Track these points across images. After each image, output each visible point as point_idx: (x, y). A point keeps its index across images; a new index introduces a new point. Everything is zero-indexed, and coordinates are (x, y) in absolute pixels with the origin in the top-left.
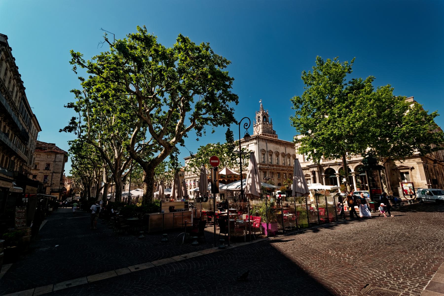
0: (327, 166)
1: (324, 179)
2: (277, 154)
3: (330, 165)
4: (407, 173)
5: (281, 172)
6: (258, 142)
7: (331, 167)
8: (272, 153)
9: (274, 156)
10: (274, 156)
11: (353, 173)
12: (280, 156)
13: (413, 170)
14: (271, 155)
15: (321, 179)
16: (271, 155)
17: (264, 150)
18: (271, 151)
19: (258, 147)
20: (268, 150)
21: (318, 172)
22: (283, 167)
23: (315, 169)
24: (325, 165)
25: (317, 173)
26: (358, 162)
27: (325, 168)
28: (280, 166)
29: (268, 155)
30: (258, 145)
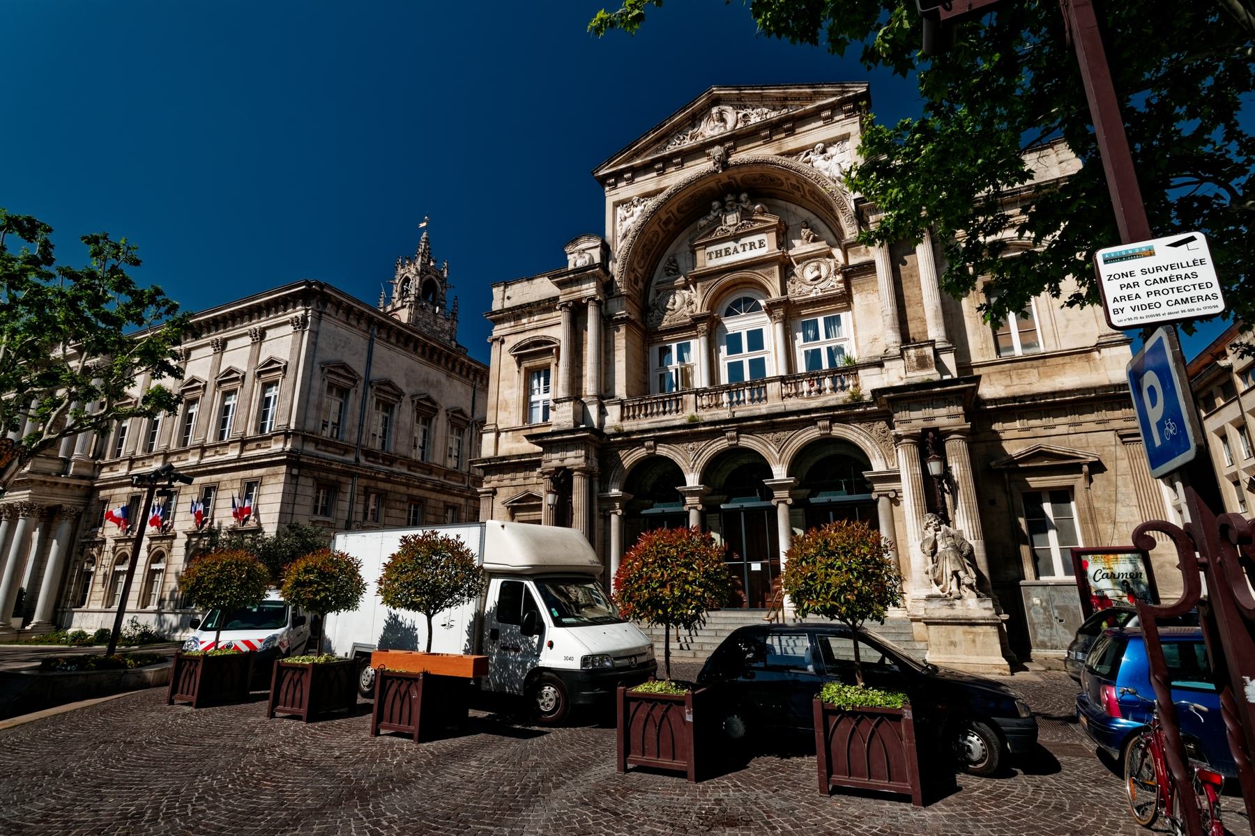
0: (640, 443)
1: (614, 519)
2: (426, 410)
3: (659, 440)
4: (1062, 496)
5: (434, 495)
6: (318, 318)
7: (662, 450)
8: (399, 394)
9: (405, 414)
10: (405, 414)
11: (781, 487)
12: (441, 423)
13: (1096, 477)
14: (388, 407)
15: (598, 522)
16: (388, 407)
17: (344, 366)
18: (389, 383)
19: (313, 345)
20: (376, 374)
21: (586, 473)
22: (448, 473)
23: (574, 459)
24: (630, 440)
25: (578, 482)
26: (813, 422)
27: (628, 459)
28: (430, 469)
29: (371, 402)
30: (314, 334)
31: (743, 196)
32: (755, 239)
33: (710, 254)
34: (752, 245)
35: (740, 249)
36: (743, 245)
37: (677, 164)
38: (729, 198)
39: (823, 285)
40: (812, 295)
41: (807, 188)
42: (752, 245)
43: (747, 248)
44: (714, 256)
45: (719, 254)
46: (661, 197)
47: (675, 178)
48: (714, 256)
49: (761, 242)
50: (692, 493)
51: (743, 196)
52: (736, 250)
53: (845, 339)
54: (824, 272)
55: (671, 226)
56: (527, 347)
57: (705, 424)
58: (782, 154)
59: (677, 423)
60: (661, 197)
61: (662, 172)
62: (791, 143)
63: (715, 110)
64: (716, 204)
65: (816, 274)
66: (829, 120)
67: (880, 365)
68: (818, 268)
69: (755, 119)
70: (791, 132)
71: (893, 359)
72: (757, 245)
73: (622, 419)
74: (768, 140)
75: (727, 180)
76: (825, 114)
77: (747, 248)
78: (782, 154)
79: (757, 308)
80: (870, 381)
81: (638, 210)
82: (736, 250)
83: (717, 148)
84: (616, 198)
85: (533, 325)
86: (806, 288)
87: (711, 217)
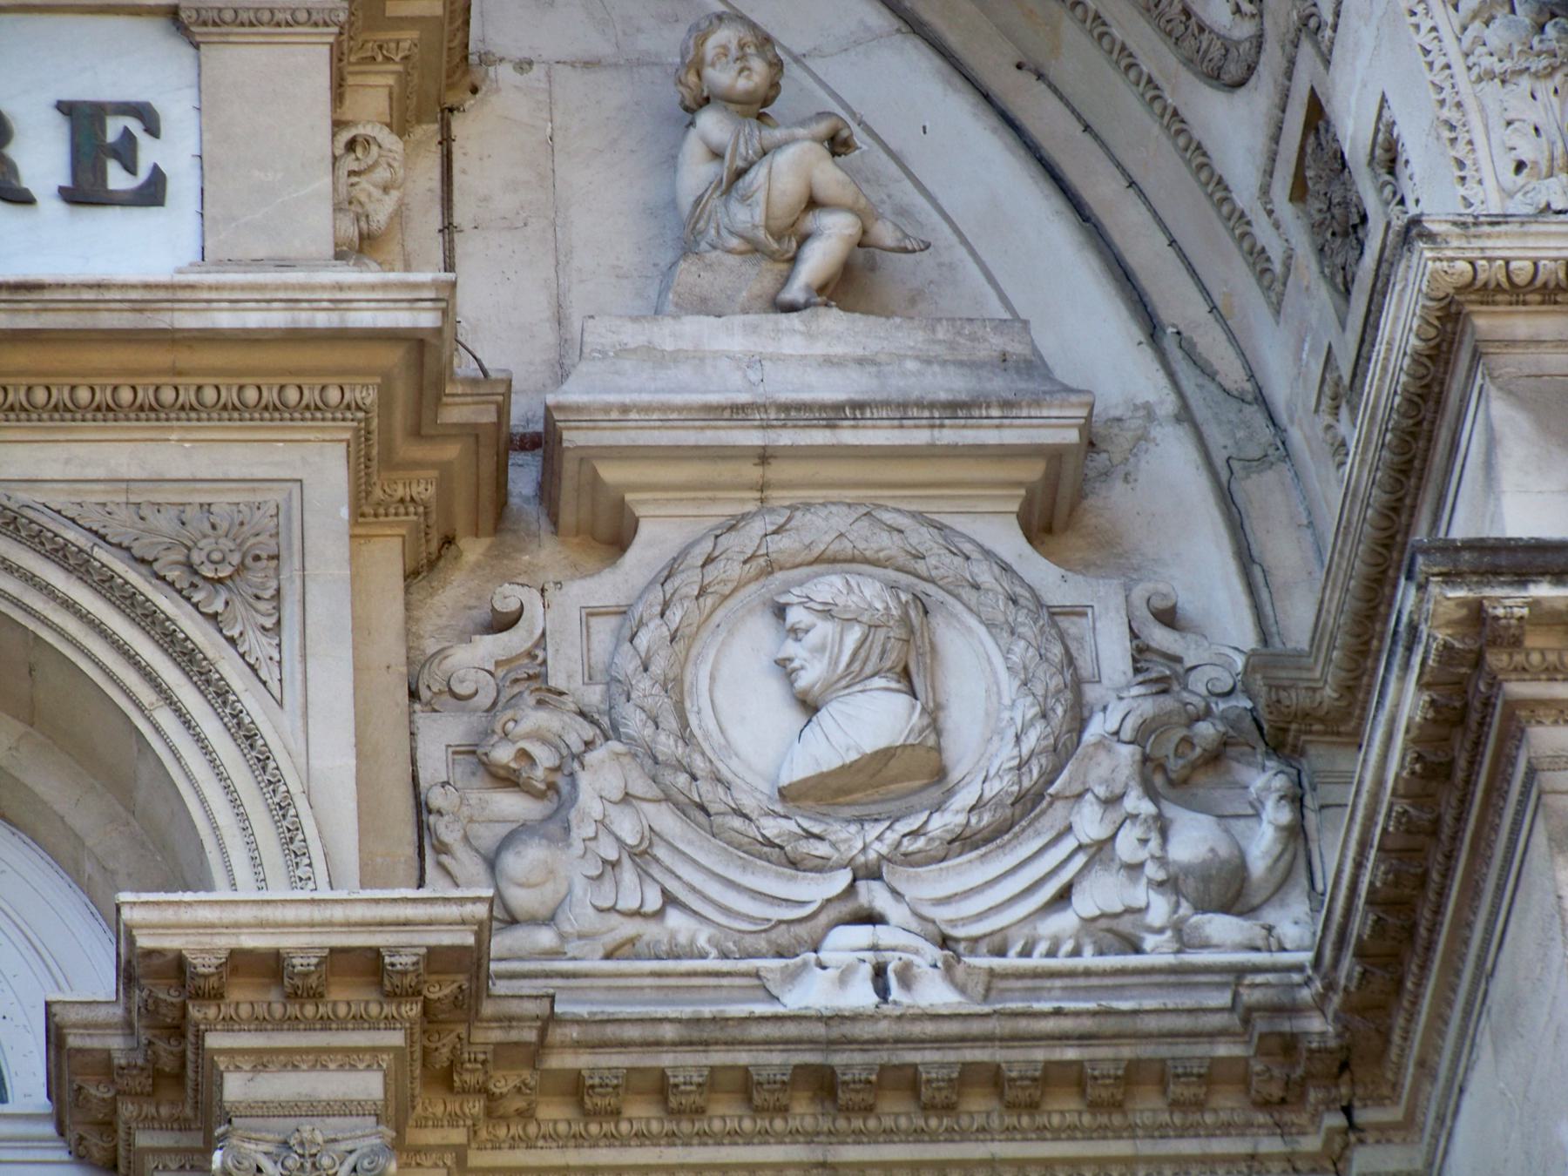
54: (986, 704)
65: (872, 720)
86: (729, 895)
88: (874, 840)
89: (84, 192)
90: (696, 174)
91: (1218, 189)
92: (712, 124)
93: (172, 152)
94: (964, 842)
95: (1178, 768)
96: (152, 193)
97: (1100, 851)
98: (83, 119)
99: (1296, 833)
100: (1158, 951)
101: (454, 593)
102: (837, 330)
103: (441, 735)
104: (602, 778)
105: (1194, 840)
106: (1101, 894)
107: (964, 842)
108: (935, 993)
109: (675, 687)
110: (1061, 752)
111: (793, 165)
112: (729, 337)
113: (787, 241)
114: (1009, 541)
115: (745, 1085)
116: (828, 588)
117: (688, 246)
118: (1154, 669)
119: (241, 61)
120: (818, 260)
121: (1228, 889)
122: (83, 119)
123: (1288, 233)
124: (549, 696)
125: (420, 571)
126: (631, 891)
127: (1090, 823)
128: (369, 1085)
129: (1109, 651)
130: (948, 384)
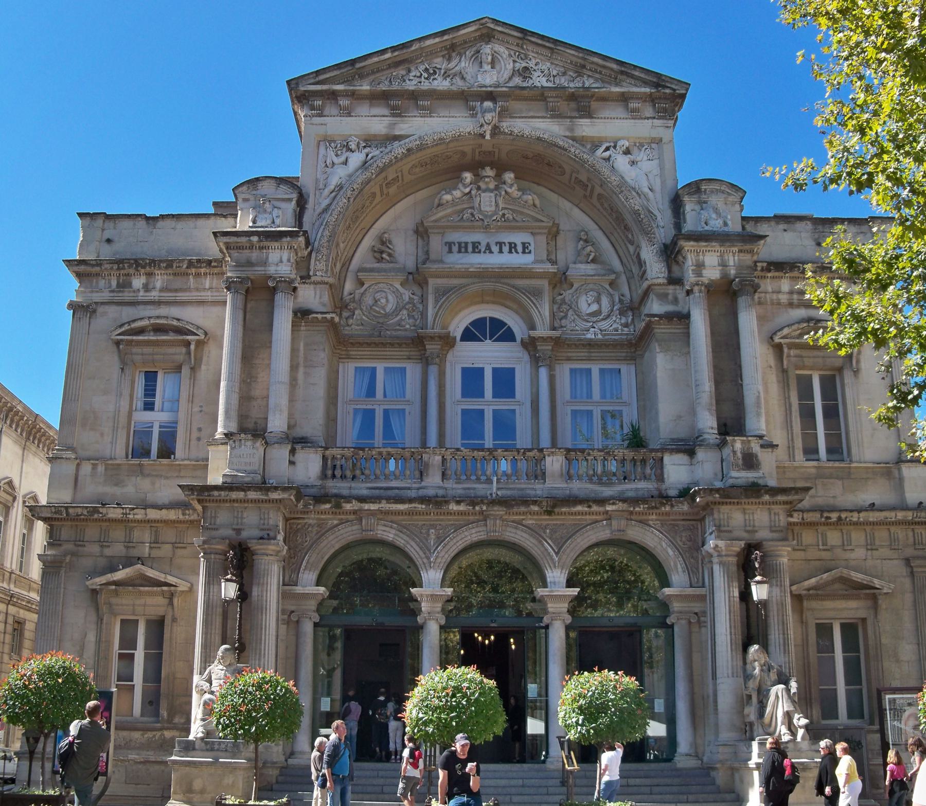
31: (509, 176)
32: (518, 238)
33: (450, 245)
34: (512, 247)
35: (495, 249)
36: (500, 244)
37: (424, 108)
38: (489, 172)
39: (604, 325)
40: (590, 336)
41: (598, 190)
42: (512, 247)
43: (506, 249)
44: (455, 248)
45: (463, 248)
46: (398, 149)
47: (421, 127)
48: (455, 248)
49: (525, 246)
50: (433, 598)
51: (509, 176)
52: (488, 249)
53: (625, 404)
55: (393, 190)
56: (141, 331)
57: (458, 503)
58: (574, 139)
59: (413, 494)
60: (398, 149)
61: (397, 112)
62: (586, 128)
63: (487, 49)
64: (468, 176)
65: (595, 307)
66: (635, 114)
67: (691, 453)
68: (598, 300)
69: (539, 80)
70: (588, 113)
71: (709, 446)
72: (520, 249)
73: (324, 476)
74: (556, 115)
75: (490, 149)
76: (633, 105)
77: (506, 249)
78: (574, 139)
79: (508, 336)
80: (677, 472)
81: (356, 159)
82: (488, 249)
83: (488, 104)
84: (321, 130)
85: (154, 295)
86: (582, 325)
87: (457, 193)
88: (595, 319)
89: (524, 252)
90: (580, 247)
91: (629, 252)
92: (581, 242)
93: (532, 248)
94: (603, 319)
95: (622, 313)
96: (530, 252)
97: (615, 321)
98: (523, 244)
99: (633, 319)
100: (620, 332)
101: (556, 290)
102: (593, 266)
103: (556, 307)
104: (570, 312)
105: (623, 321)
106: (615, 326)
107: (603, 319)
108: (600, 336)
109: (577, 302)
110: (612, 310)
111: (589, 248)
112: (582, 266)
113: (589, 255)
114: (608, 287)
115: (583, 345)
116: (591, 293)
117: (579, 255)
118: (621, 301)
119: (539, 237)
120: (591, 258)
121: (626, 325)
122: (523, 244)
123: (635, 259)
124: (566, 303)
125: (554, 288)
126: (573, 325)
127: (614, 318)
128: (550, 348)
129: (617, 299)
130: (603, 272)
